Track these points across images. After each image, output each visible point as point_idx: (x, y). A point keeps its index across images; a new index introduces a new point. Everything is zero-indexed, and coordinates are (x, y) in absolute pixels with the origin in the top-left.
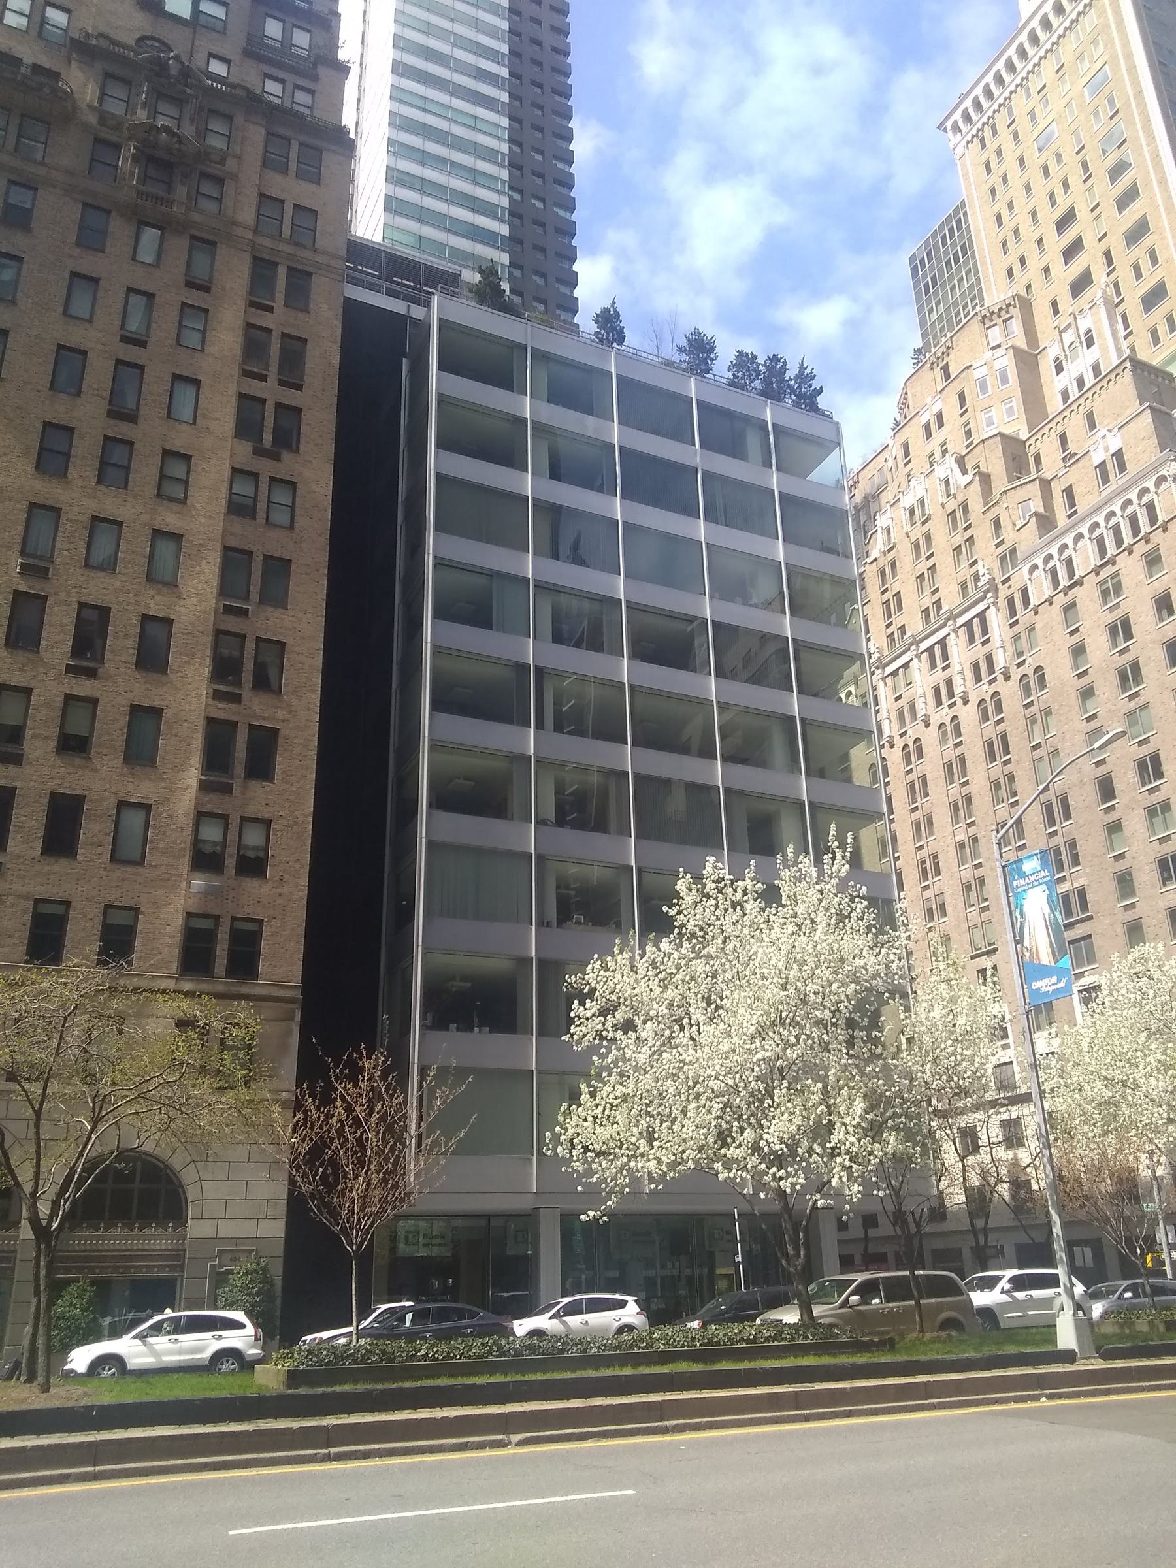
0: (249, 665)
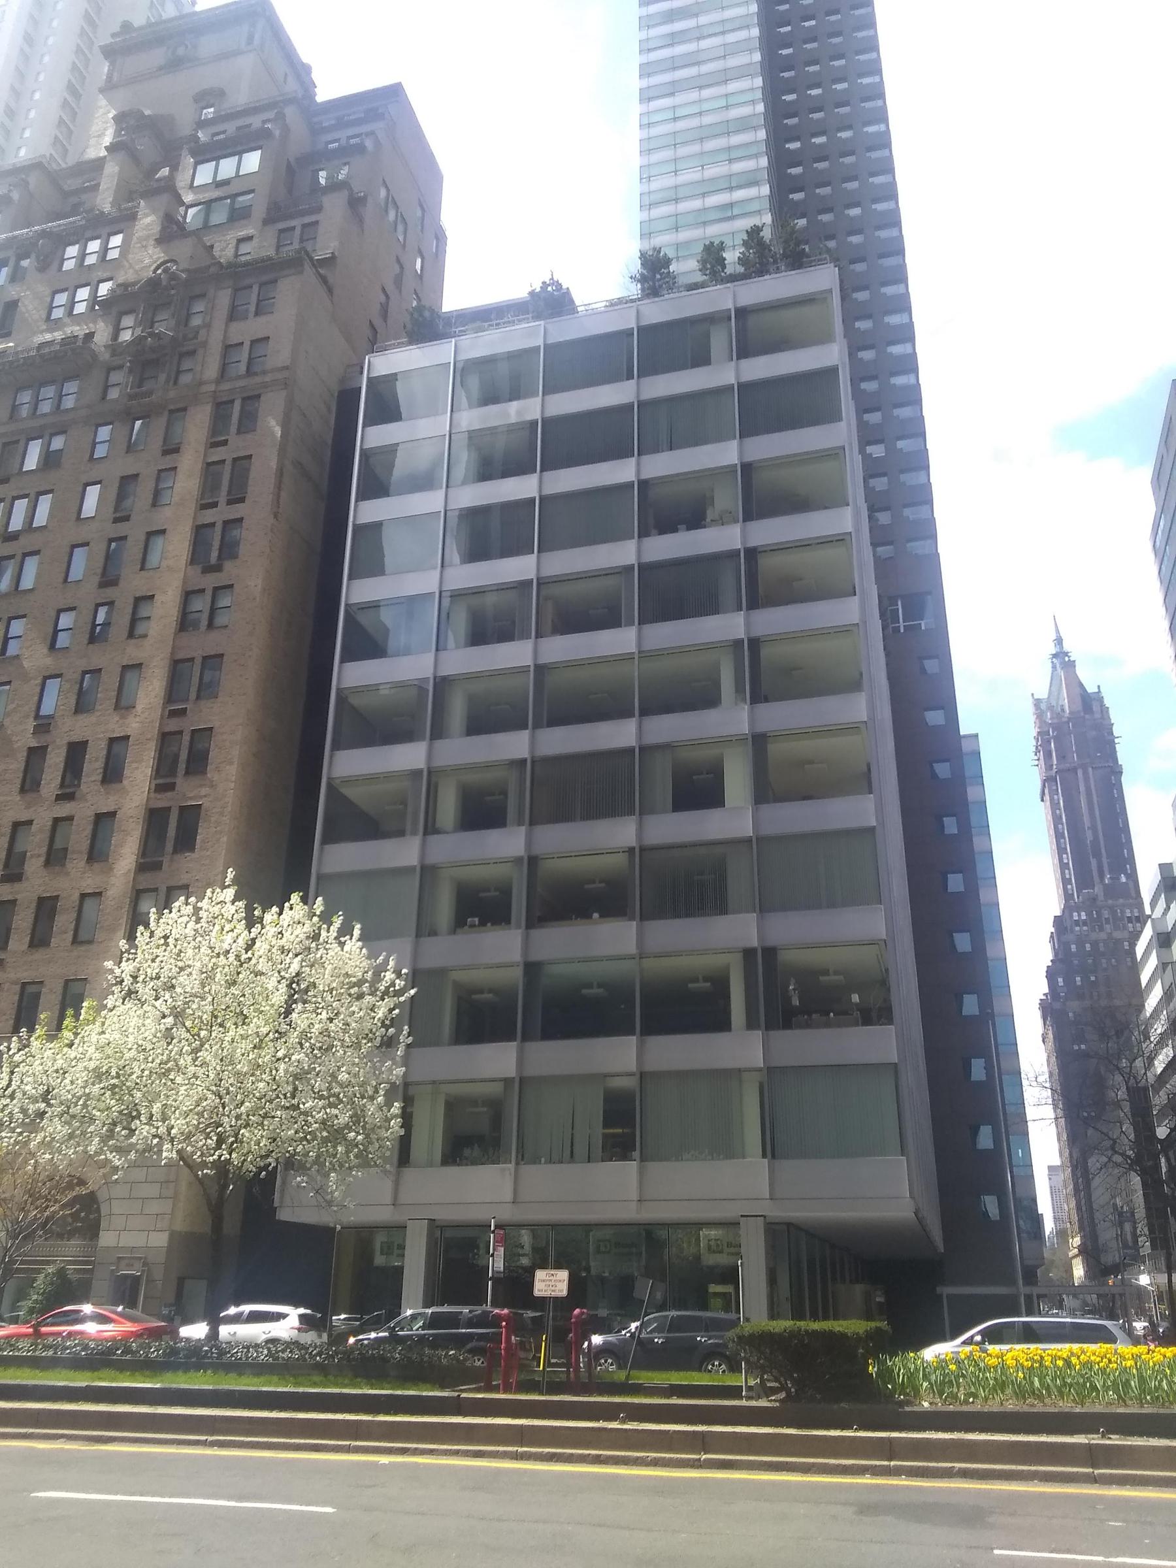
0: (184, 756)
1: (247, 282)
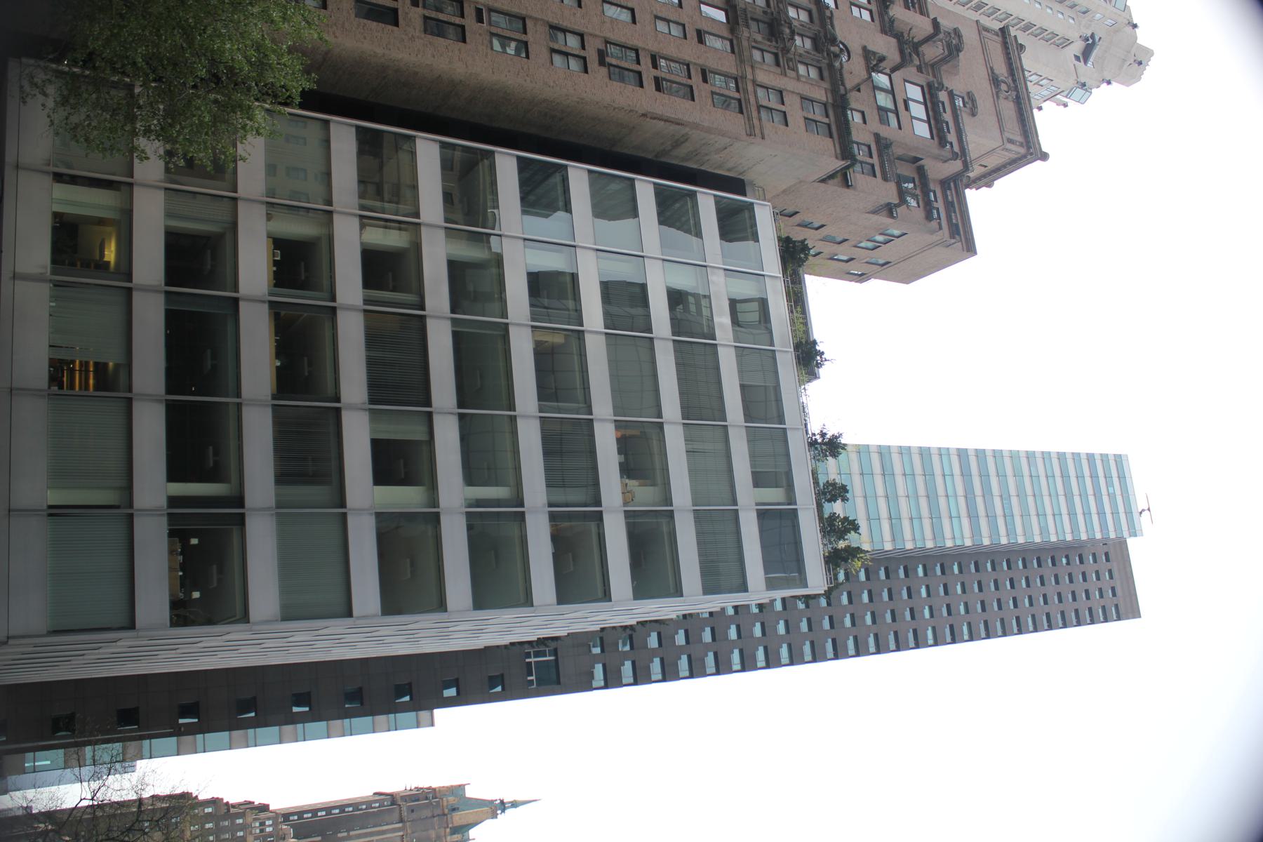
0: (441, 16)
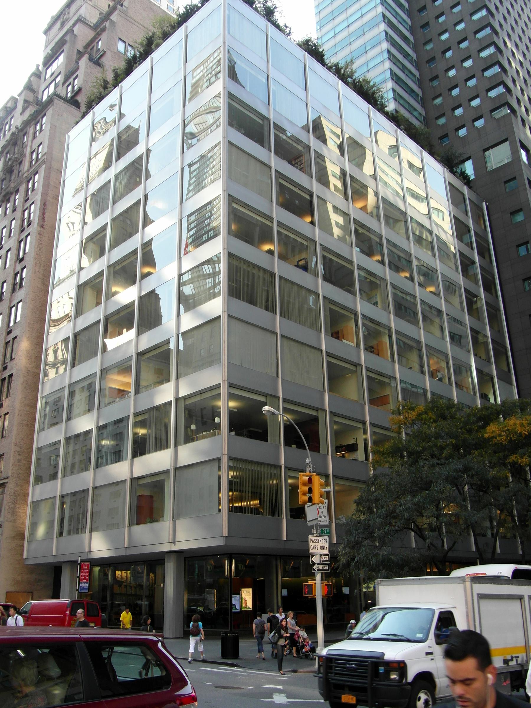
1: (37, 120)
